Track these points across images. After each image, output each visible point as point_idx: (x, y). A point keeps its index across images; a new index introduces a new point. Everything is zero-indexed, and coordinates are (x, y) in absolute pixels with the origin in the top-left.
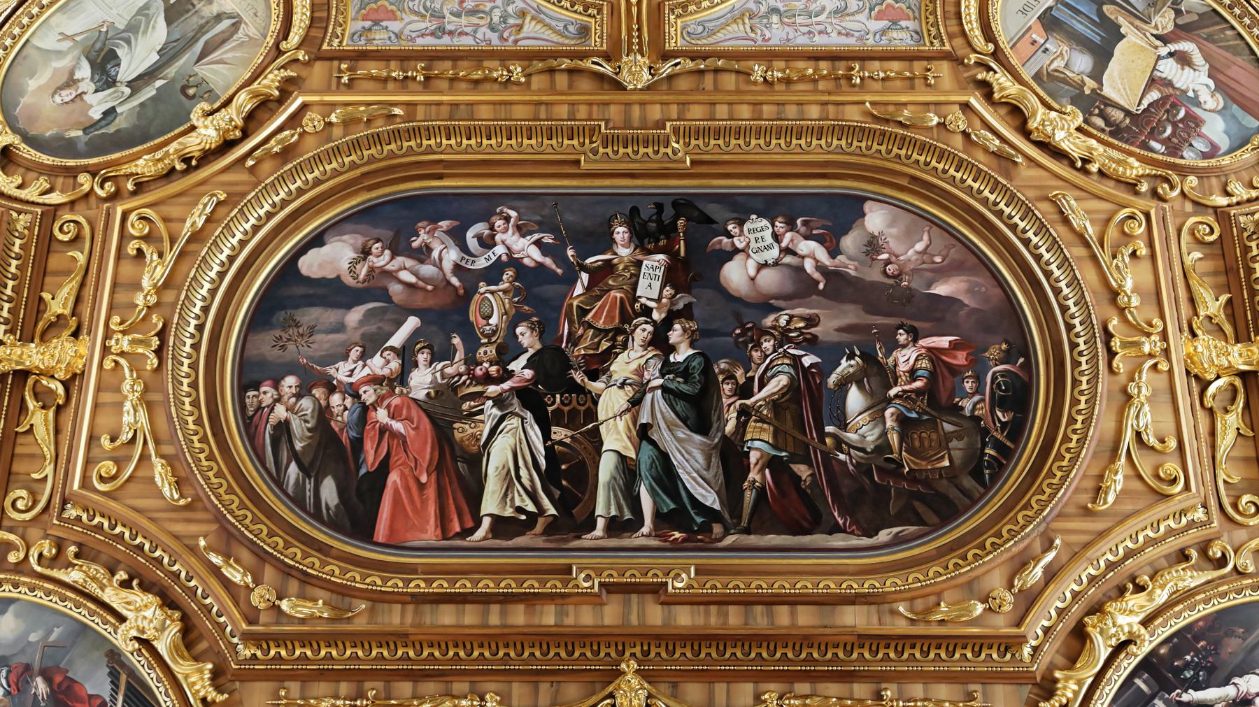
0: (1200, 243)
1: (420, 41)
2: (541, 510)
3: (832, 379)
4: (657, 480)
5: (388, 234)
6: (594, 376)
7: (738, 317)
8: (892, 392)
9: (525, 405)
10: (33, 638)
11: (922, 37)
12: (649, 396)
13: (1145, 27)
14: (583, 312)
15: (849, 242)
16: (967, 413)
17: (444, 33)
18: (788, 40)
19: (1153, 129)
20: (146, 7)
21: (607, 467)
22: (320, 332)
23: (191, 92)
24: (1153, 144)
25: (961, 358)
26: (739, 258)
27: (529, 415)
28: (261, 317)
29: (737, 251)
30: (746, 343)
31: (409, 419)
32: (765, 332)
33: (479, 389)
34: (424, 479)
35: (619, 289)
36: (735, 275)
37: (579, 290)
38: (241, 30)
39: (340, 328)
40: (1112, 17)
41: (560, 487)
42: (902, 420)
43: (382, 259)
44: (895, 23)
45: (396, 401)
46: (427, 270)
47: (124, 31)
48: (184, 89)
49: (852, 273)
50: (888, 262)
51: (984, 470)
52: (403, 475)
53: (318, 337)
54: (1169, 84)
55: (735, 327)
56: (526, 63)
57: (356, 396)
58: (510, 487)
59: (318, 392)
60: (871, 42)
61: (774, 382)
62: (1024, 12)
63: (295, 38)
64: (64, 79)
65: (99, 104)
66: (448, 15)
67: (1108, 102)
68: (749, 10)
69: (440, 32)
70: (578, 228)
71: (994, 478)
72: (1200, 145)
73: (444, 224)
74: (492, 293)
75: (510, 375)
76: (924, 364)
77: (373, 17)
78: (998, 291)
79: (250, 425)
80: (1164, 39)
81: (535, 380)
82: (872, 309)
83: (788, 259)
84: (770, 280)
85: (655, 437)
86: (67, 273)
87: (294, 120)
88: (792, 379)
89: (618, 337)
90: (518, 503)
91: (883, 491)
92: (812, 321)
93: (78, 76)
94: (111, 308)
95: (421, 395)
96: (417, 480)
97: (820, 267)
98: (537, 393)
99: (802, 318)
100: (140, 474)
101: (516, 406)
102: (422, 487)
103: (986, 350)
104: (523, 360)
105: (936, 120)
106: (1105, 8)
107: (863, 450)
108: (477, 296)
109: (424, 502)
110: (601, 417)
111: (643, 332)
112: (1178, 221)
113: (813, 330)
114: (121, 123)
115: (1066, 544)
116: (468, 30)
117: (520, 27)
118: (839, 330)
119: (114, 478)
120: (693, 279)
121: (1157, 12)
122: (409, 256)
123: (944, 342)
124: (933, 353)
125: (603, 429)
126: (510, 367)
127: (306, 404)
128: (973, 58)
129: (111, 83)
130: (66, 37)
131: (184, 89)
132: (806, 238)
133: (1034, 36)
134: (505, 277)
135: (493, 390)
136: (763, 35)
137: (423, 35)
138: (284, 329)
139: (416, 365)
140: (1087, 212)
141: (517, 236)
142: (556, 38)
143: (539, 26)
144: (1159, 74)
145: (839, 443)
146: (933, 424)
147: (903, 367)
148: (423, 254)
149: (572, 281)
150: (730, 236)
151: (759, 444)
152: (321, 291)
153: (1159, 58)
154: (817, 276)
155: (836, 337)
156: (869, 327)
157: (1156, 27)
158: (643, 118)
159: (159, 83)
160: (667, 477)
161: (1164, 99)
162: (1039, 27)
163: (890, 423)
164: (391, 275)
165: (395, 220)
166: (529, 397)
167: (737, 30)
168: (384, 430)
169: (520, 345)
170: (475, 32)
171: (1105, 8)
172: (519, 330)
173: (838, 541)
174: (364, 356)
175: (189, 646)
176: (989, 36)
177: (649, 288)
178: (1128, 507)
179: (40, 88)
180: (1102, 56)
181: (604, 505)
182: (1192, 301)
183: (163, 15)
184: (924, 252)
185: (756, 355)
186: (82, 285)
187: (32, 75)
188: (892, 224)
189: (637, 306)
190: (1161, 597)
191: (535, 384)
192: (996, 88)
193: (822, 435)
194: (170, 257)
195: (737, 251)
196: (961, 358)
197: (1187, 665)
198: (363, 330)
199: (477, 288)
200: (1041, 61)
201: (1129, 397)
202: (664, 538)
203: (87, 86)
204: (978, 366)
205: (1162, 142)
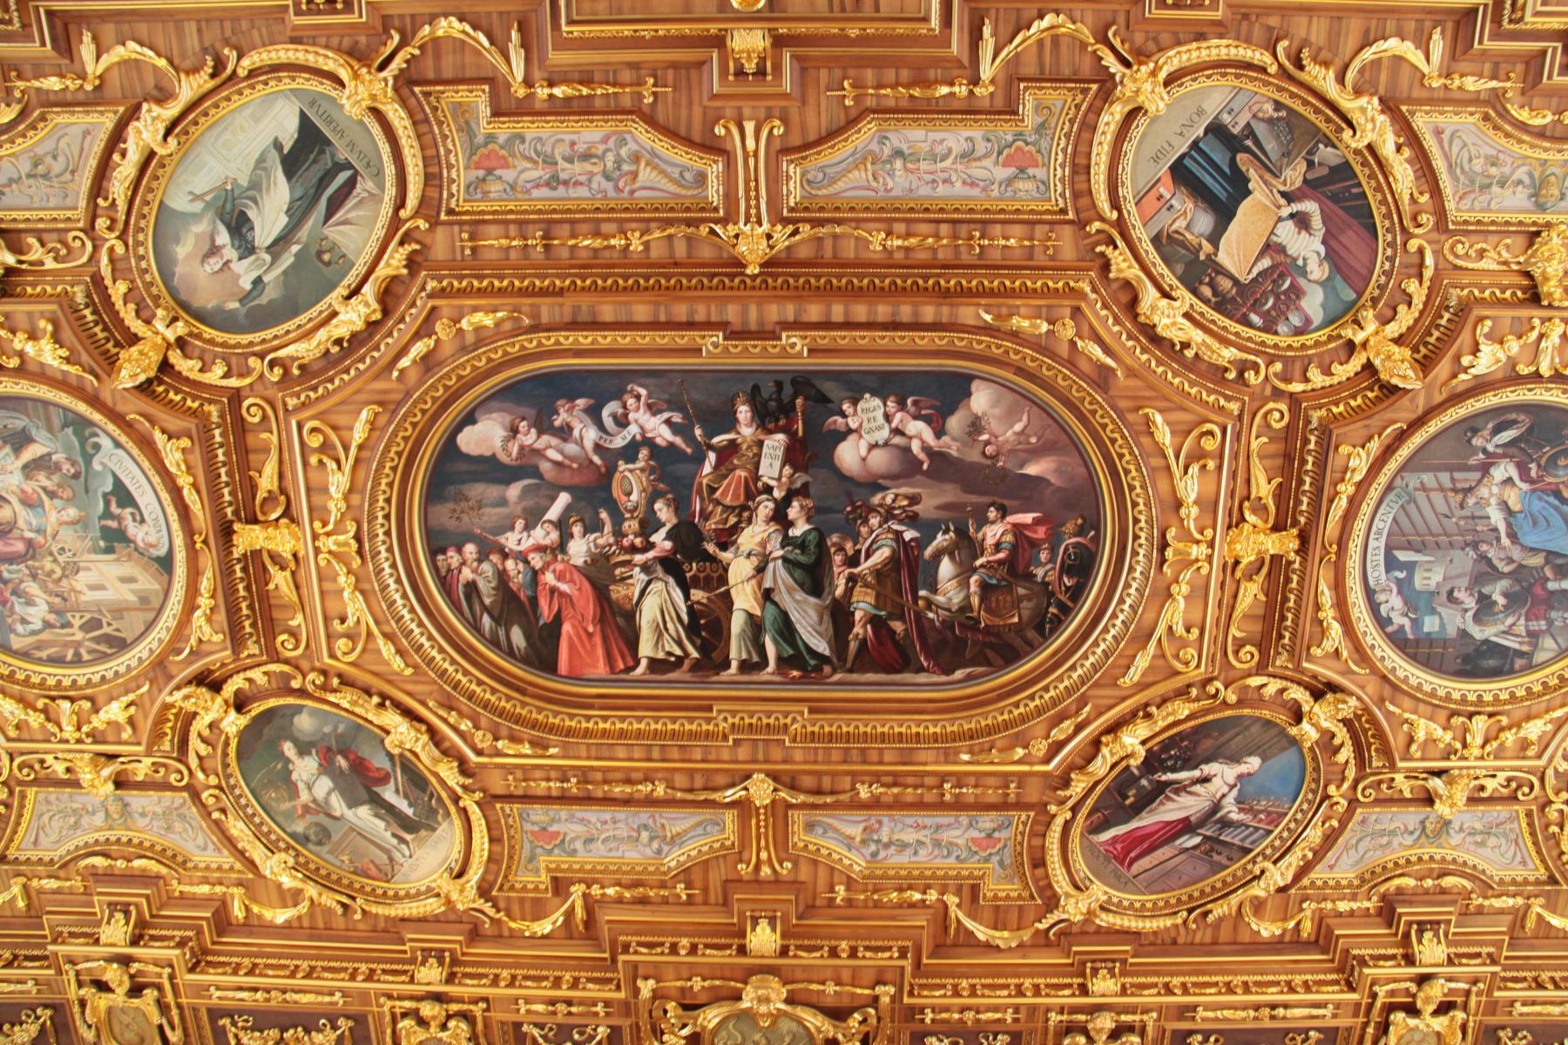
0: (1269, 426)
1: (536, 193)
2: (687, 655)
3: (928, 552)
4: (780, 633)
5: (531, 412)
6: (724, 547)
7: (849, 494)
8: (978, 563)
9: (668, 571)
10: (327, 730)
11: (1048, 188)
12: (771, 565)
13: (1274, 182)
14: (712, 490)
15: (955, 423)
16: (1039, 579)
17: (558, 183)
18: (911, 190)
19: (1256, 301)
20: (261, 160)
21: (737, 623)
22: (487, 505)
23: (326, 257)
24: (1255, 318)
25: (1041, 533)
26: (852, 438)
27: (671, 580)
28: (437, 490)
29: (850, 431)
30: (855, 520)
31: (572, 581)
32: (872, 509)
33: (627, 557)
34: (591, 629)
35: (743, 467)
36: (848, 455)
37: (707, 469)
39: (503, 502)
40: (1244, 169)
41: (700, 636)
42: (985, 587)
43: (529, 438)
44: (1022, 170)
45: (559, 567)
46: (571, 448)
47: (248, 189)
49: (954, 453)
50: (988, 443)
51: (1045, 626)
52: (573, 626)
53: (487, 510)
54: (1281, 249)
55: (845, 503)
56: (643, 226)
57: (527, 562)
58: (660, 636)
59: (495, 558)
60: (995, 194)
61: (878, 554)
62: (1156, 159)
64: (207, 247)
65: (247, 271)
66: (560, 161)
67: (1221, 270)
68: (871, 152)
69: (554, 182)
70: (703, 403)
71: (1052, 632)
72: (1296, 320)
73: (581, 402)
74: (631, 471)
75: (652, 546)
76: (1009, 538)
77: (486, 164)
78: (1083, 470)
79: (446, 582)
80: (1289, 197)
81: (674, 551)
82: (968, 489)
83: (897, 440)
84: (880, 461)
85: (777, 599)
86: (267, 451)
87: (425, 329)
88: (894, 551)
89: (744, 512)
90: (668, 648)
91: (960, 643)
92: (914, 500)
94: (311, 510)
95: (579, 562)
96: (586, 630)
97: (926, 449)
98: (677, 561)
99: (906, 497)
100: (370, 646)
101: (660, 572)
102: (590, 635)
103: (1063, 525)
104: (662, 533)
105: (1045, 327)
106: (1239, 157)
107: (949, 610)
108: (617, 475)
109: (593, 647)
110: (731, 581)
111: (765, 508)
112: (1256, 404)
113: (915, 508)
114: (270, 294)
115: (1095, 707)
116: (582, 179)
117: (635, 174)
118: (939, 508)
119: (353, 650)
120: (810, 458)
121: (1288, 165)
122: (554, 435)
123: (1028, 518)
124: (1018, 529)
125: (733, 592)
126: (653, 538)
127: (486, 566)
128: (1097, 225)
129: (247, 249)
130: (197, 198)
131: (319, 254)
132: (915, 418)
133: (1162, 190)
134: (640, 456)
135: (639, 558)
136: (885, 184)
137: (538, 186)
138: (456, 501)
139: (572, 536)
140: (1169, 424)
141: (648, 415)
142: (672, 188)
143: (655, 173)
144: (1274, 238)
145: (930, 604)
146: (1010, 588)
147: (990, 541)
148: (565, 433)
149: (701, 460)
150: (844, 416)
151: (863, 604)
152: (480, 468)
153: (1280, 219)
154: (922, 456)
155: (934, 515)
156: (964, 505)
157: (1284, 183)
158: (761, 322)
159: (295, 248)
160: (786, 630)
161: (1273, 268)
162: (1168, 180)
163: (973, 588)
164: (539, 453)
165: (538, 396)
166: (670, 565)
167: (859, 177)
168: (553, 590)
169: (659, 520)
170: (590, 181)
171: (1239, 157)
172: (657, 506)
173: (922, 678)
174: (528, 527)
175: (437, 745)
176: (1115, 204)
177: (771, 467)
178: (1150, 679)
179: (189, 256)
180: (1224, 213)
181: (737, 651)
182: (1248, 481)
183: (280, 169)
184: (1022, 433)
185: (864, 530)
186: (281, 462)
187: (177, 241)
188: (994, 405)
189: (760, 484)
190: (1161, 724)
191: (675, 553)
192: (1113, 268)
193: (916, 598)
194: (347, 468)
195: (850, 431)
196: (1041, 533)
197: (1171, 757)
198: (524, 504)
199: (615, 467)
200: (1164, 221)
201: (1170, 595)
202: (785, 675)
203: (230, 253)
204: (1054, 539)
205: (1265, 315)
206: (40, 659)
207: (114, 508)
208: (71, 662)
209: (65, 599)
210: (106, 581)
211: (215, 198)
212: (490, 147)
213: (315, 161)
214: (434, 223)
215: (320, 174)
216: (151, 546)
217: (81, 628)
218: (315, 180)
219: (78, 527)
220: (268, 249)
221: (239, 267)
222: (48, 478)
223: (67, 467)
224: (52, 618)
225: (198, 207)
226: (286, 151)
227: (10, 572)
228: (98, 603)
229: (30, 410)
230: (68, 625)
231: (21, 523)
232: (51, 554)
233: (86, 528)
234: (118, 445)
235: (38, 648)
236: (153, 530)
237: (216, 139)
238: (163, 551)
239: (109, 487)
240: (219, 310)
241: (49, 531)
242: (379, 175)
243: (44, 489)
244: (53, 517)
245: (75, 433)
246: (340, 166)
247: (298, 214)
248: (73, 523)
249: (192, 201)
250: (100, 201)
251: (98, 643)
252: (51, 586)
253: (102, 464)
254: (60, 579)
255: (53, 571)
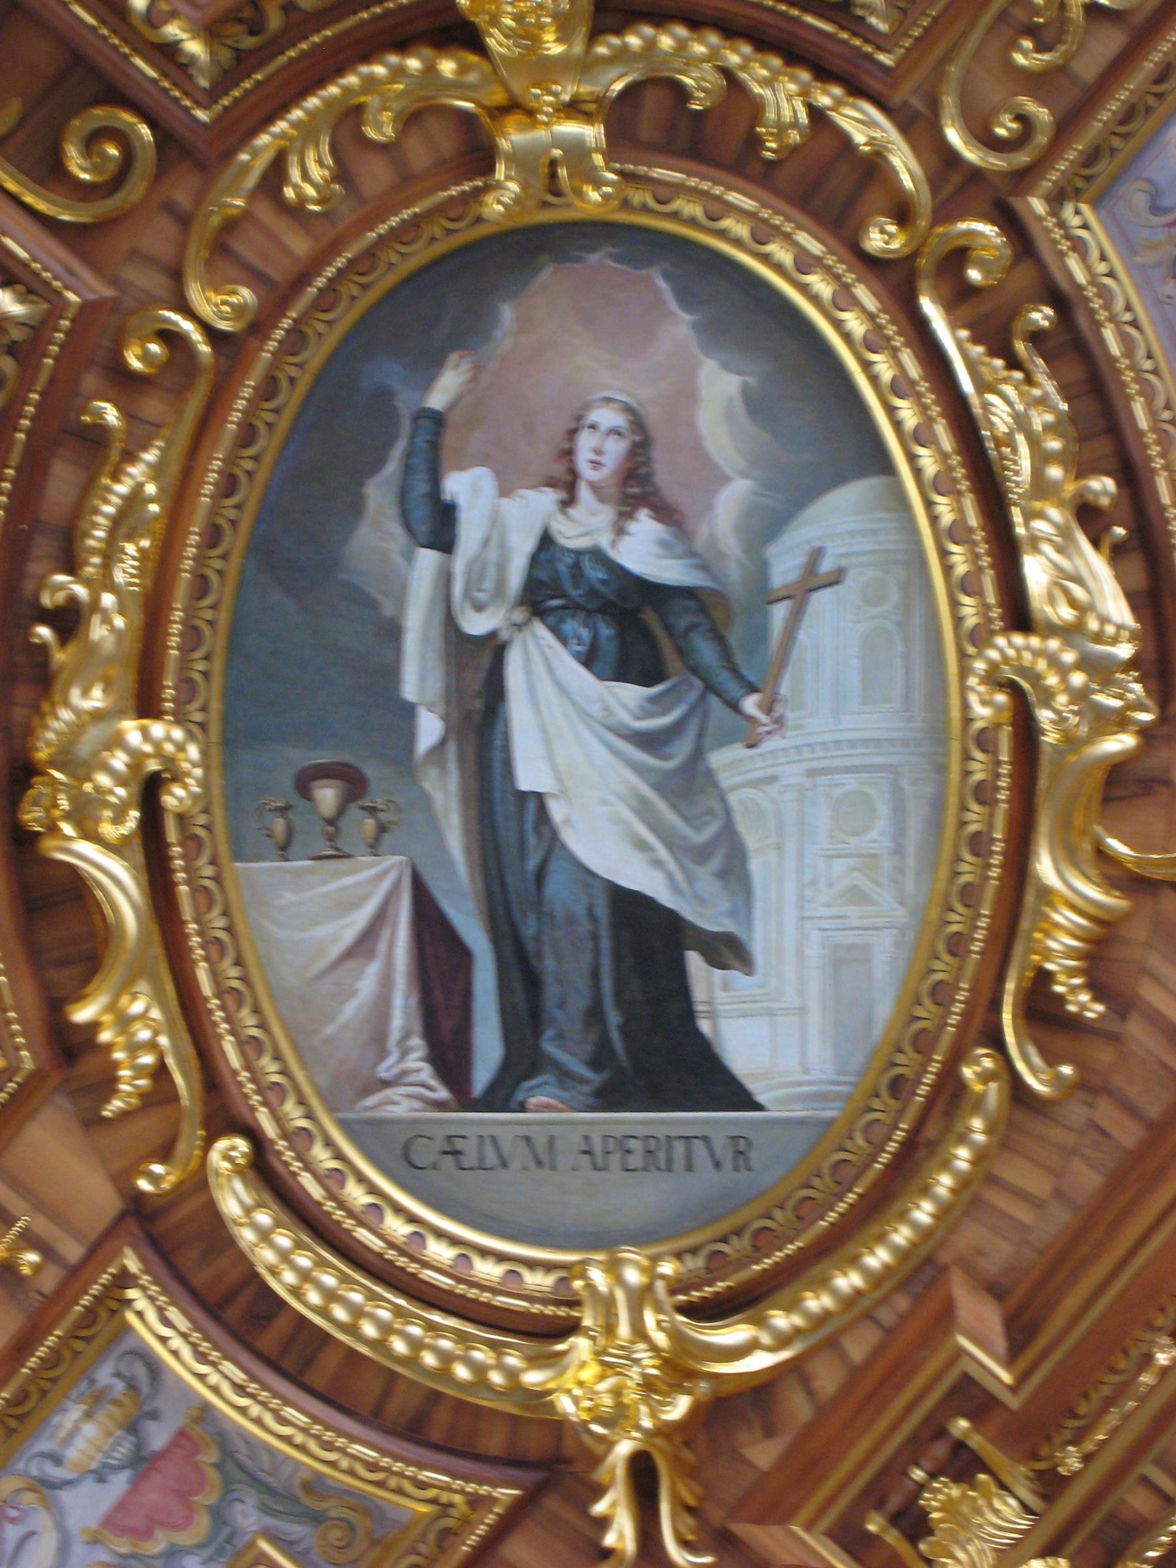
23: (327, 795)
38: (426, 1073)
47: (698, 754)
48: (354, 784)
63: (234, 1199)
65: (496, 521)
93: (645, 526)
130: (814, 580)
131: (354, 784)
159: (429, 728)
179: (687, 395)
183: (664, 896)
203: (586, 526)
211: (760, 635)
212: (203, 1522)
213: (595, 1014)
214: (141, 1217)
215: (551, 991)
218: (549, 963)
220: (494, 650)
221: (533, 508)
225: (784, 567)
226: (694, 960)
237: (897, 793)
240: (469, 332)
242: (403, 1156)
246: (523, 1064)
247: (508, 835)
249: (817, 555)
250: (1042, 316)
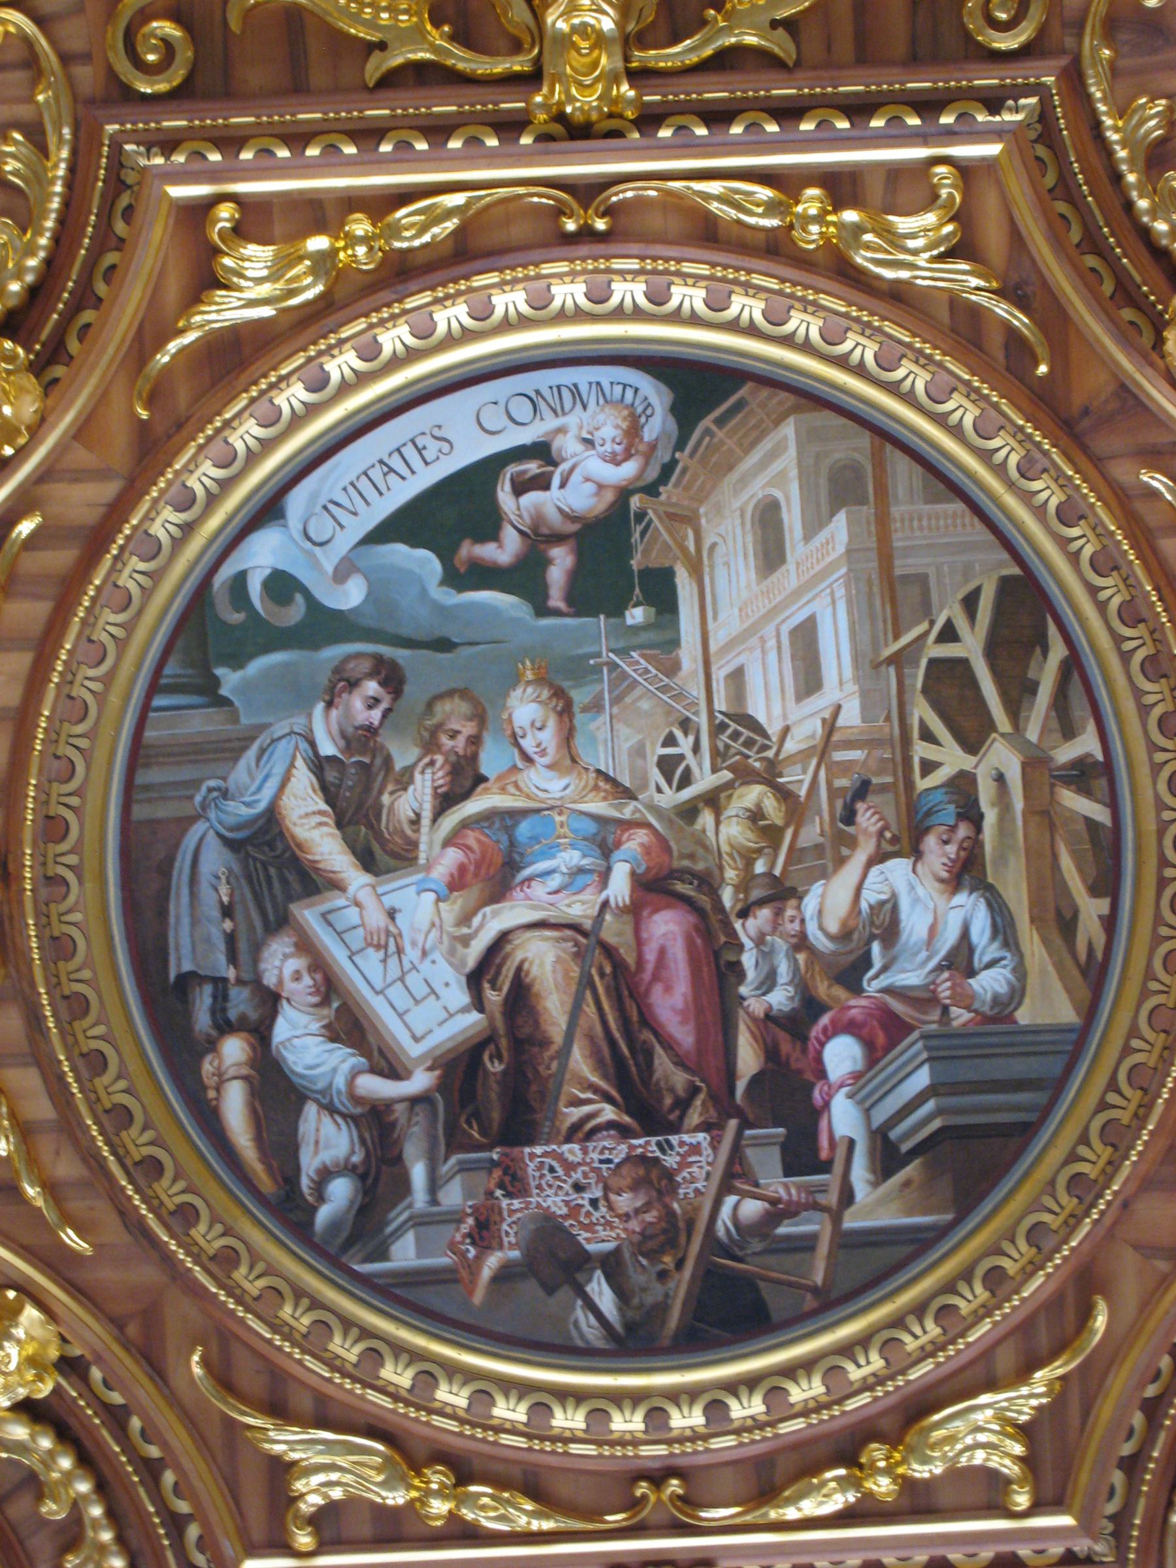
206: (1110, 923)
207: (505, 550)
208: (1114, 805)
209: (863, 790)
210: (780, 622)
216: (633, 431)
217: (972, 744)
219: (580, 696)
222: (405, 780)
223: (362, 705)
224: (938, 853)
227: (769, 982)
228: (870, 665)
229: (162, 811)
230: (962, 787)
231: (579, 908)
232: (689, 812)
233: (582, 668)
234: (268, 510)
235: (1067, 924)
236: (574, 419)
238: (653, 393)
239: (423, 562)
241: (598, 806)
243: (445, 801)
244: (546, 783)
245: (237, 661)
248: (566, 712)
251: (1032, 688)
252: (811, 834)
253: (341, 575)
254: (784, 794)
255: (755, 816)
